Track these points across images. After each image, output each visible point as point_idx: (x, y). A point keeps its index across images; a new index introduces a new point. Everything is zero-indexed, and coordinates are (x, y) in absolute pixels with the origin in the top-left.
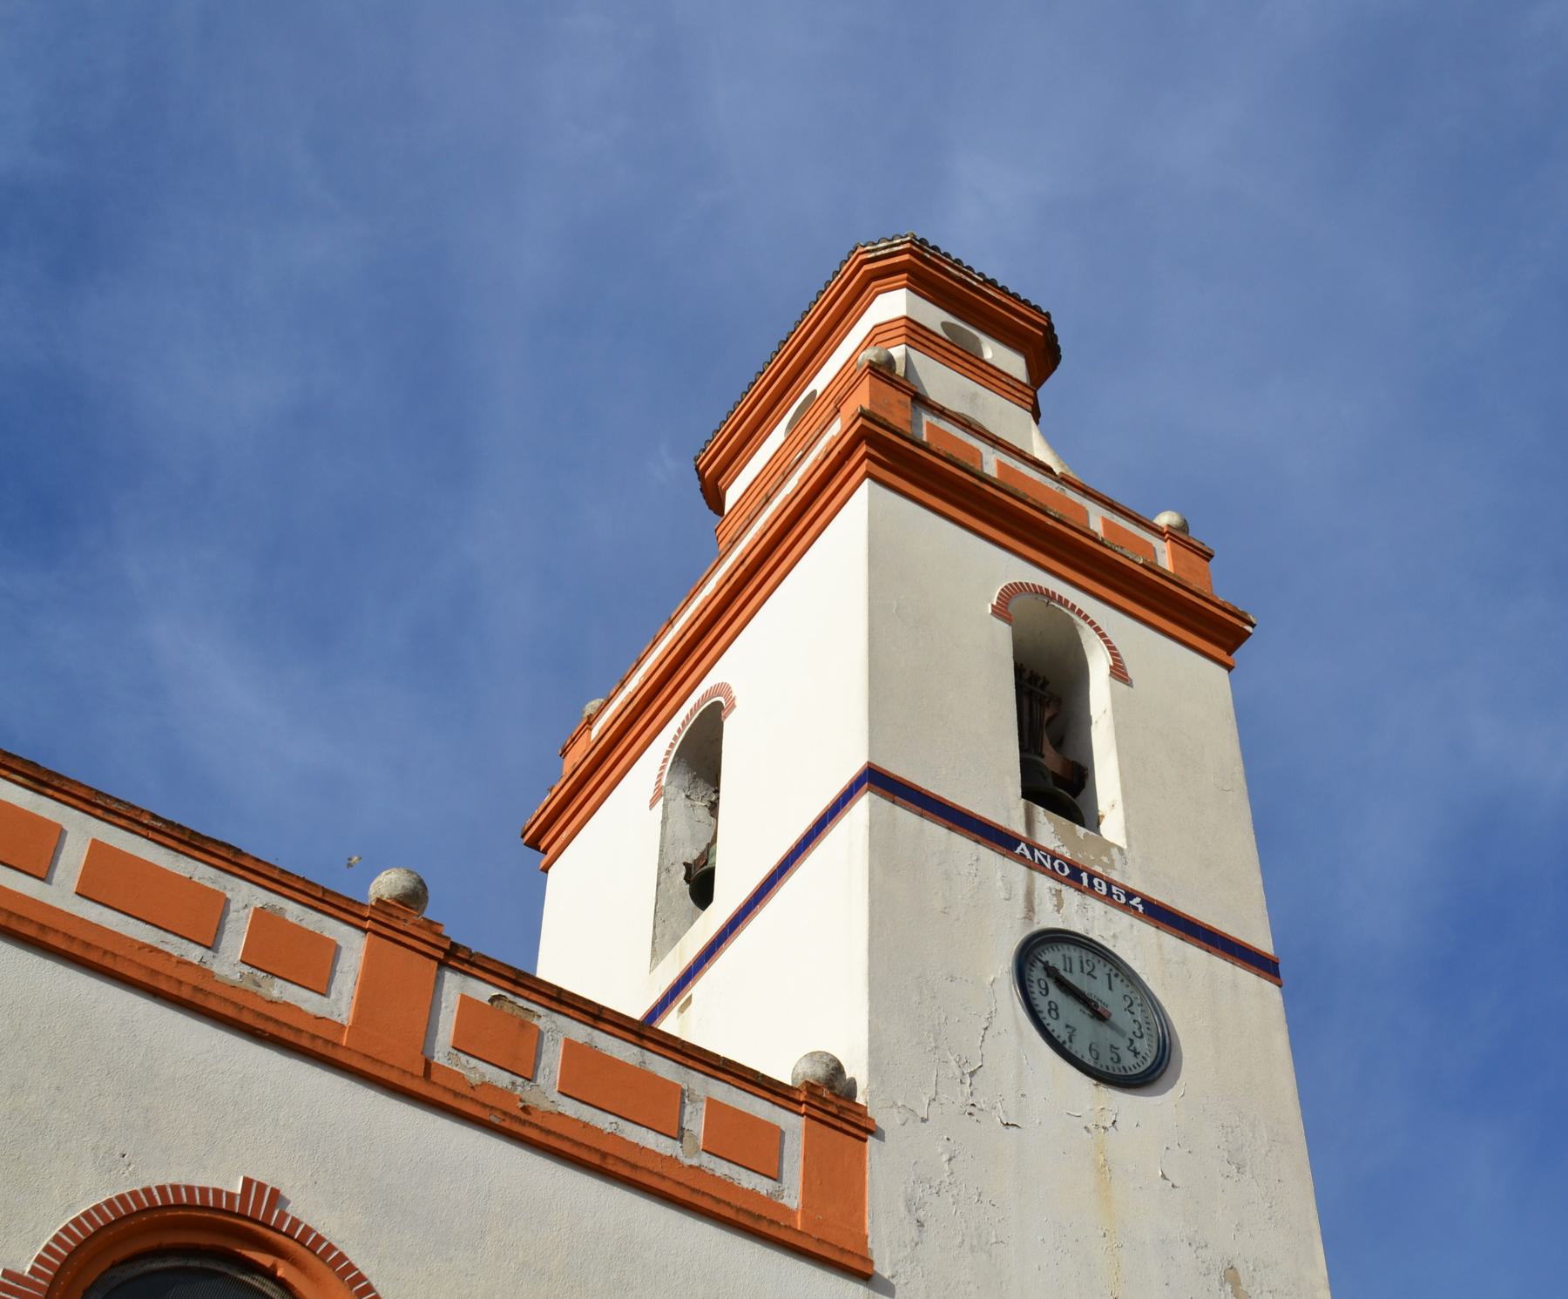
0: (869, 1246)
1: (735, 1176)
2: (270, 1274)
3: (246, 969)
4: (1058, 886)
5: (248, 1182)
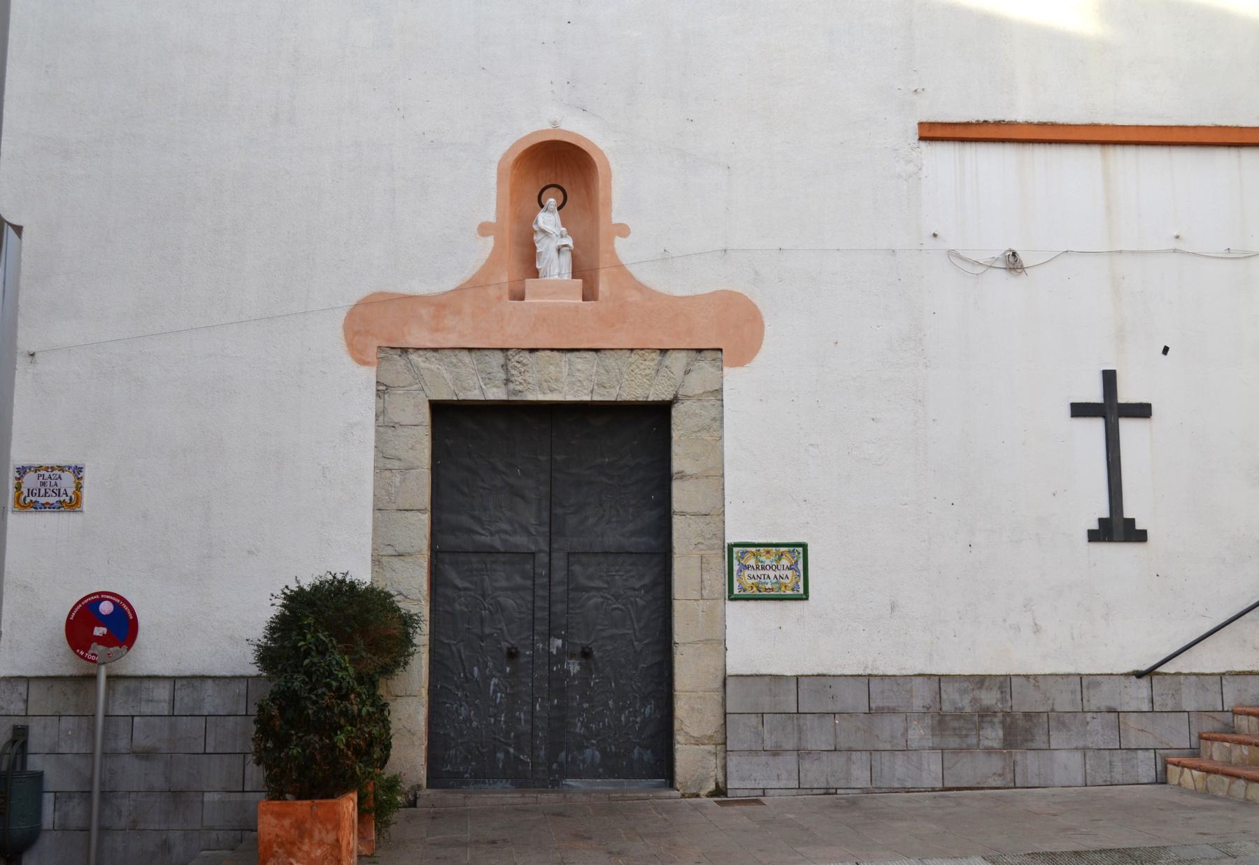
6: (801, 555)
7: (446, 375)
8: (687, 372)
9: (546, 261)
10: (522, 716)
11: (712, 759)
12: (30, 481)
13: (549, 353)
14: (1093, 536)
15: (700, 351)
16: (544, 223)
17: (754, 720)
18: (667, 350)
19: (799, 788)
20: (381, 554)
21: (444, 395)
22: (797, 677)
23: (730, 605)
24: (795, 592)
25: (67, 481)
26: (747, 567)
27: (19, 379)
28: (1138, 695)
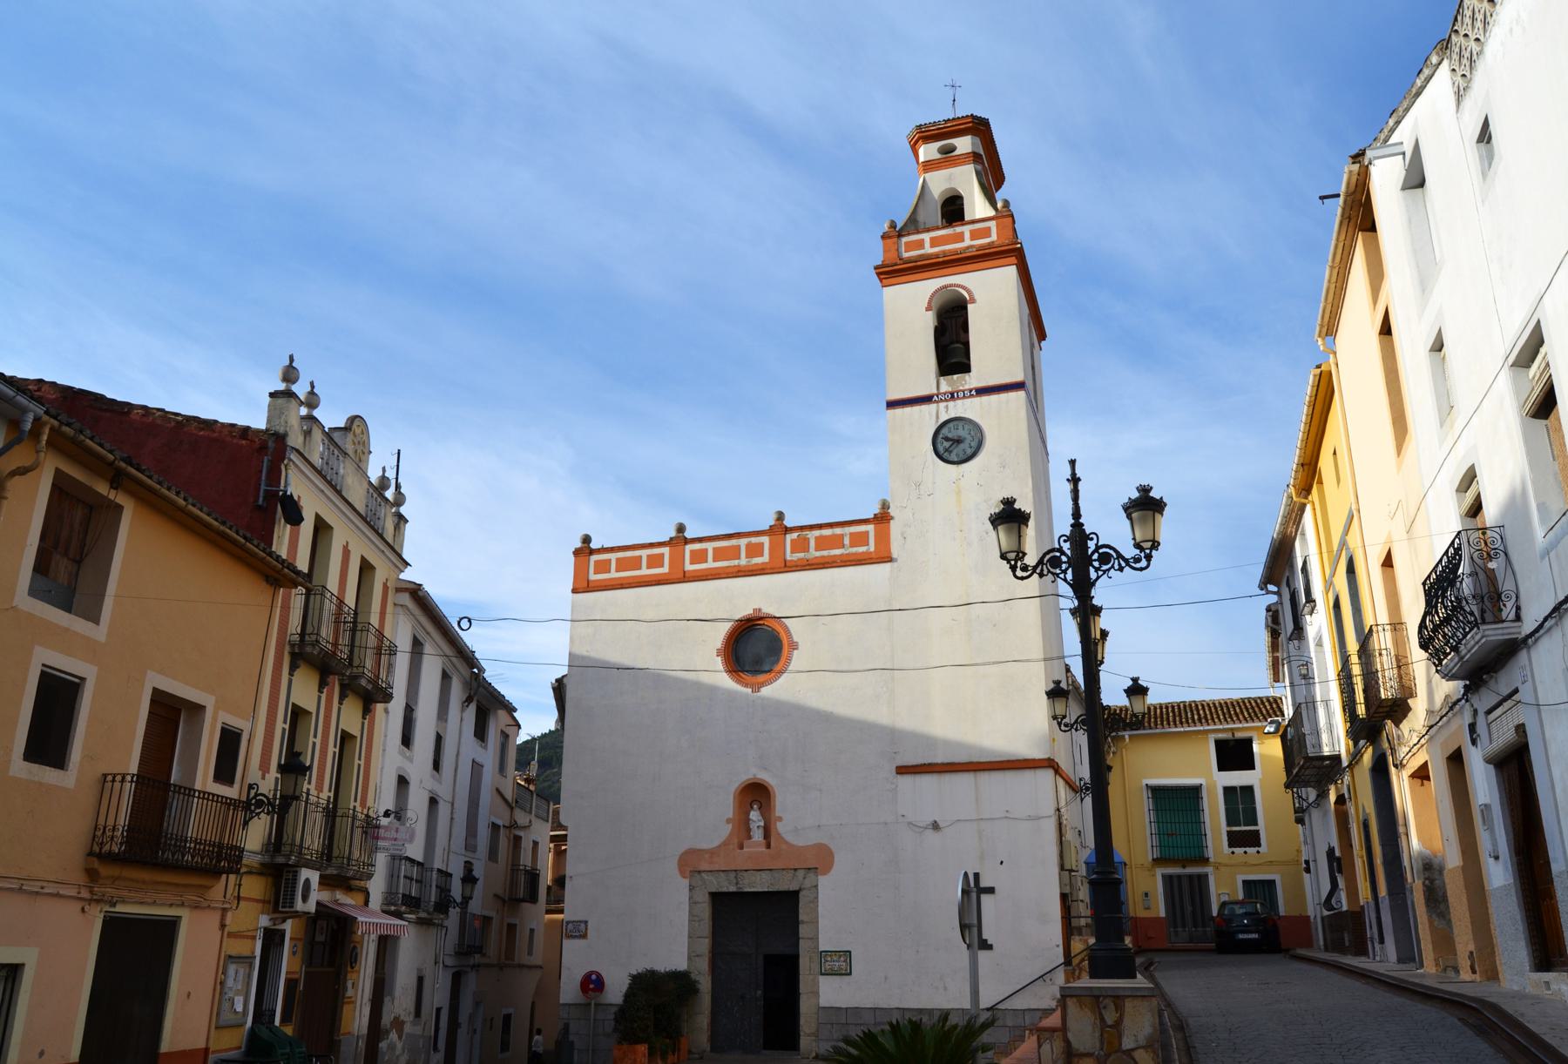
4: (945, 404)
8: (804, 878)
11: (814, 1044)
15: (809, 869)
17: (829, 1026)
21: (714, 890)
22: (847, 1008)
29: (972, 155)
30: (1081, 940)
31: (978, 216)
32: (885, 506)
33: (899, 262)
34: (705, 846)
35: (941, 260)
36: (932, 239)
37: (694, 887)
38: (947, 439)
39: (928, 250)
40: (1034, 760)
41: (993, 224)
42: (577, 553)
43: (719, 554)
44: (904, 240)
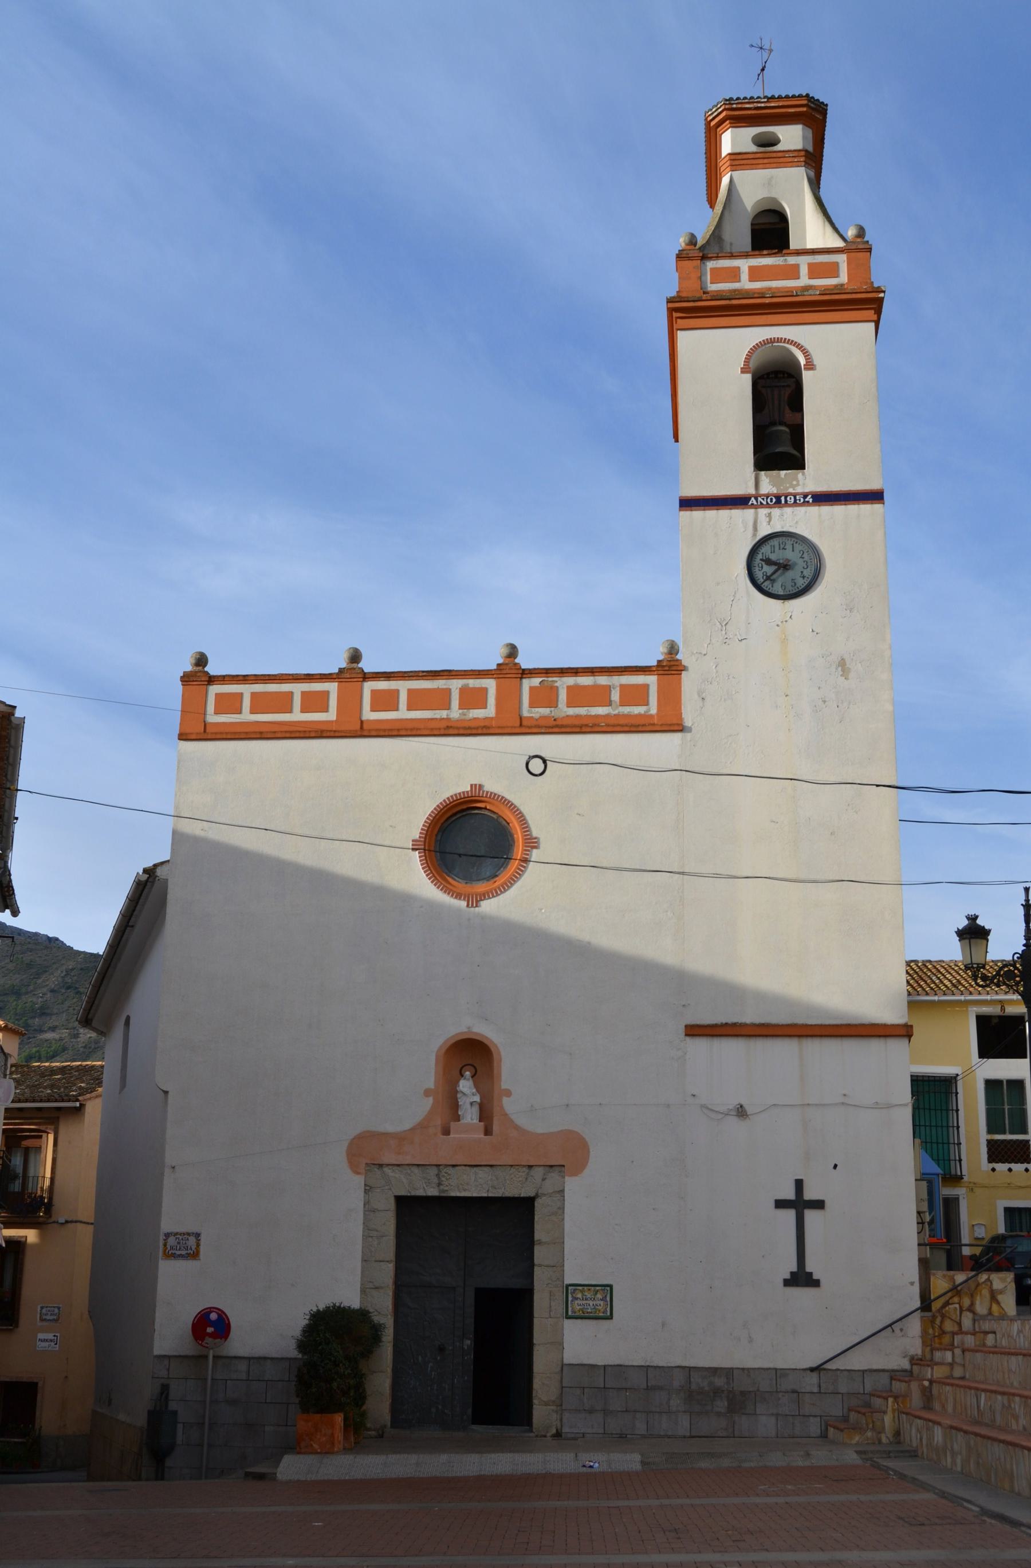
0: (683, 716)
1: (632, 710)
2: (486, 808)
3: (461, 711)
5: (471, 785)
6: (609, 1292)
7: (404, 1181)
8: (544, 1180)
9: (464, 1110)
10: (447, 1387)
11: (555, 1416)
12: (172, 1241)
13: (464, 1168)
14: (787, 1283)
15: (551, 1166)
16: (463, 1087)
18: (532, 1166)
19: (604, 1433)
20: (366, 1287)
21: (403, 1193)
22: (605, 1366)
23: (565, 1320)
24: (605, 1314)
25: (192, 1241)
26: (577, 1299)
27: (165, 1182)
28: (811, 1382)
29: (803, 153)
30: (944, 1276)
31: (810, 245)
32: (673, 649)
33: (704, 297)
34: (390, 1128)
35: (767, 301)
36: (752, 270)
37: (371, 1188)
38: (768, 562)
39: (746, 284)
40: (885, 1026)
41: (842, 259)
42: (187, 679)
43: (416, 700)
44: (710, 264)
